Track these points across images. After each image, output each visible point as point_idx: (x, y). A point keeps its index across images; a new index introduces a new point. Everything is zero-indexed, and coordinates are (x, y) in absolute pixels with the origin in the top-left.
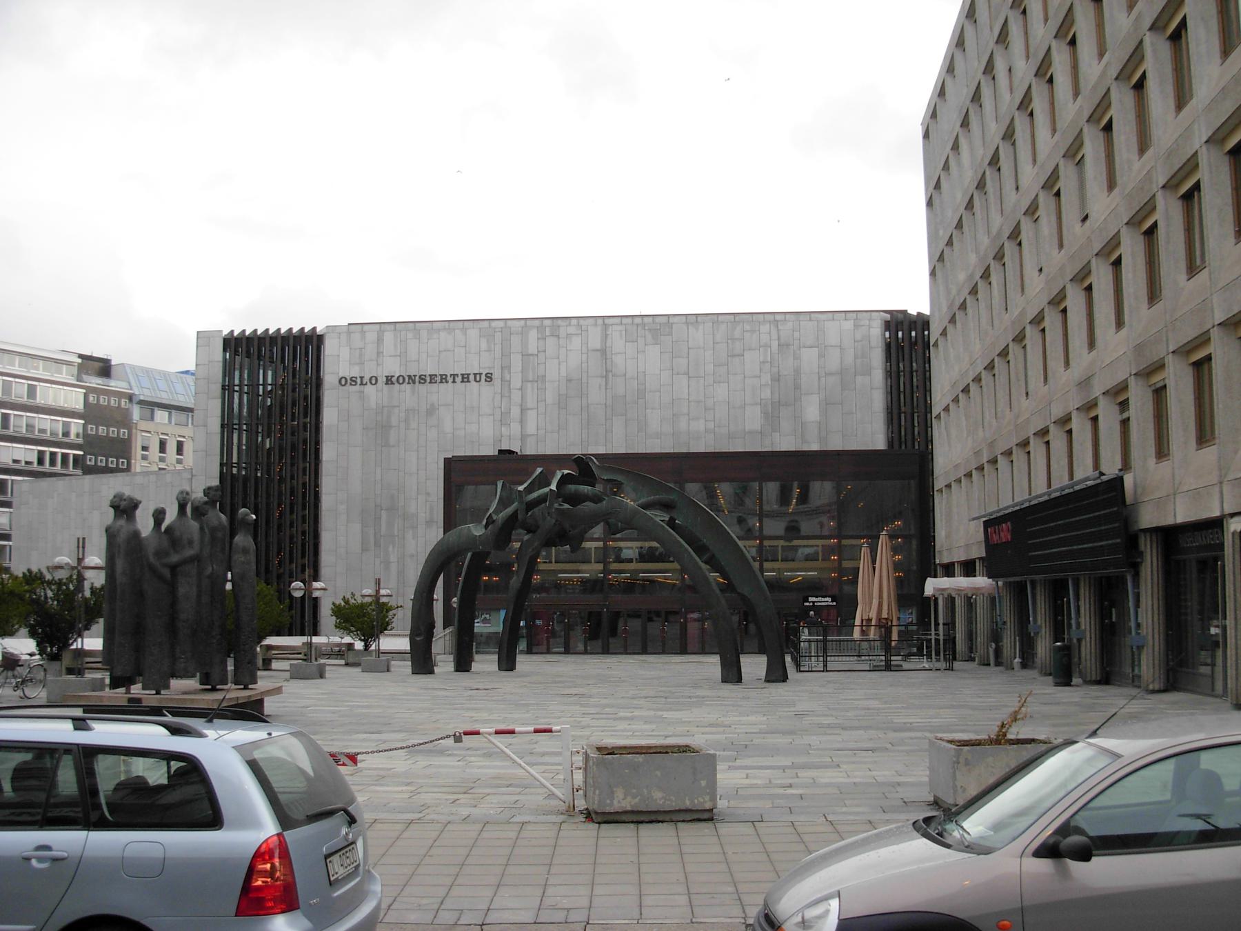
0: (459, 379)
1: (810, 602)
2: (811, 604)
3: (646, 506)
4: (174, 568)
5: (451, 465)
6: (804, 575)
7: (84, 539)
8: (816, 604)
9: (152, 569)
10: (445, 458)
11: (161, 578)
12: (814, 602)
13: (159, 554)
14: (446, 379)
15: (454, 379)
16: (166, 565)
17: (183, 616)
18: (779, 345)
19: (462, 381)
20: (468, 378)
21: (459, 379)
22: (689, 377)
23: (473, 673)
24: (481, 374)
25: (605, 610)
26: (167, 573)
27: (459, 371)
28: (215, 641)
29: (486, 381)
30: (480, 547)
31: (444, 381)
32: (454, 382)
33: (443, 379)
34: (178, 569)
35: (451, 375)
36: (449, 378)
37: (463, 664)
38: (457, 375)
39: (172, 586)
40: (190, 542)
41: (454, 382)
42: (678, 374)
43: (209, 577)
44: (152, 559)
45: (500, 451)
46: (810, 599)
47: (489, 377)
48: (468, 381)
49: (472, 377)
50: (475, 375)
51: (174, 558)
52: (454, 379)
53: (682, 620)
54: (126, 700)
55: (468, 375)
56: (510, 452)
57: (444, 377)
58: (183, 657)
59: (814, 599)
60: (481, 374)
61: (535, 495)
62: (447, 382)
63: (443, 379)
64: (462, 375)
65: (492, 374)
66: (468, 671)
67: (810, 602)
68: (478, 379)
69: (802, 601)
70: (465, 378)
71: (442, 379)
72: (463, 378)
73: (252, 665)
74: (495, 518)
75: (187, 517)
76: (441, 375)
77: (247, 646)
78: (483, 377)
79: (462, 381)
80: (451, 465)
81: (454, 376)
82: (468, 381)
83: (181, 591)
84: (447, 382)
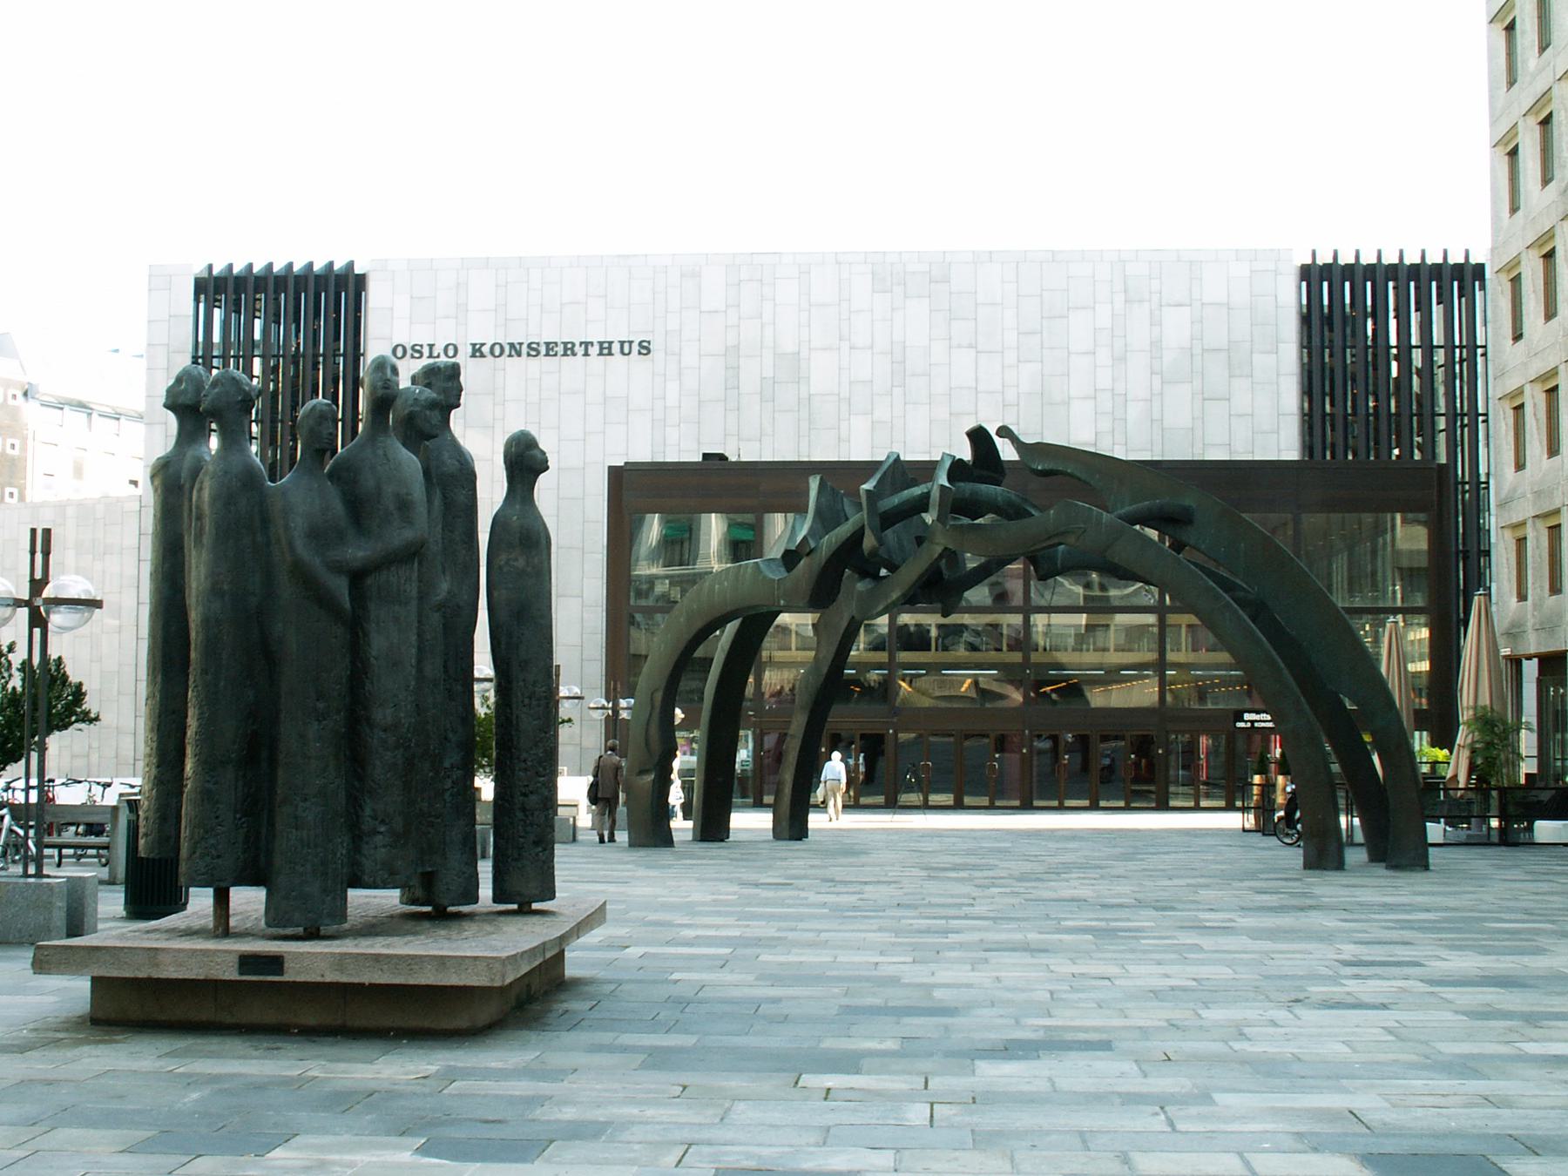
0: (594, 350)
1: (1246, 722)
2: (1249, 725)
3: (1133, 520)
4: (357, 577)
5: (618, 476)
6: (1221, 675)
7: (47, 532)
8: (1256, 725)
9: (304, 577)
10: (610, 467)
11: (323, 600)
12: (1252, 722)
13: (320, 535)
14: (572, 349)
15: (586, 349)
16: (337, 568)
17: (383, 715)
18: (1126, 301)
19: (601, 354)
20: (610, 348)
21: (594, 350)
22: (977, 352)
23: (738, 843)
24: (631, 343)
25: (891, 731)
26: (340, 587)
27: (596, 337)
28: (448, 784)
29: (640, 353)
30: (782, 602)
31: (569, 352)
32: (586, 354)
33: (569, 350)
34: (369, 581)
35: (581, 343)
36: (577, 348)
37: (713, 828)
38: (592, 344)
39: (356, 627)
40: (404, 506)
41: (586, 354)
42: (959, 346)
43: (441, 607)
44: (303, 550)
45: (705, 455)
46: (1247, 716)
47: (645, 348)
48: (610, 354)
49: (616, 348)
50: (622, 343)
51: (357, 552)
52: (586, 349)
53: (1024, 751)
54: (234, 961)
55: (611, 343)
56: (722, 457)
57: (569, 346)
58: (382, 829)
59: (1253, 716)
60: (631, 343)
61: (896, 500)
62: (574, 354)
63: (569, 350)
64: (601, 343)
65: (649, 342)
66: (722, 841)
67: (1246, 722)
68: (626, 351)
69: (1232, 719)
70: (606, 349)
71: (566, 349)
72: (602, 348)
73: (545, 850)
74: (813, 545)
75: (323, 468)
76: (565, 344)
77: (533, 798)
78: (635, 347)
79: (601, 354)
80: (618, 476)
81: (587, 345)
82: (610, 354)
83: (378, 644)
84: (574, 354)
